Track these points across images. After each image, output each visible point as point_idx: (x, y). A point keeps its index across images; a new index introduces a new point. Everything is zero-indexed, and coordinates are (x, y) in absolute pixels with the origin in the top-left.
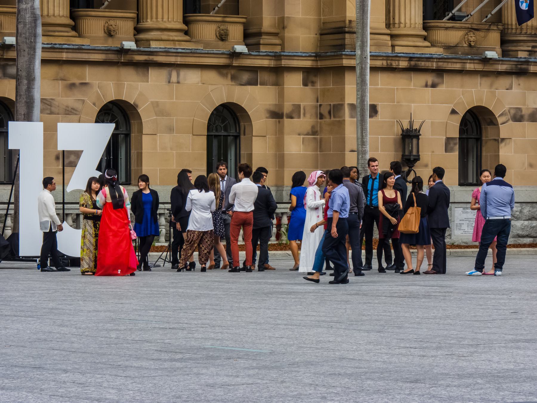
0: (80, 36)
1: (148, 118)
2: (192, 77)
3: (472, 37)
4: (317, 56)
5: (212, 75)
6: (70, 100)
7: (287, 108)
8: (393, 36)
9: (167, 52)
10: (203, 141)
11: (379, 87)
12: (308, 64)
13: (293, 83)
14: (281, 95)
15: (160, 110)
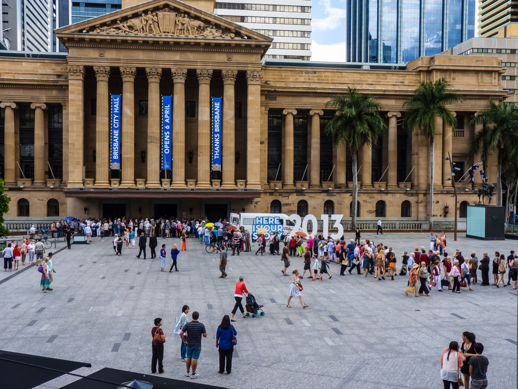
0: (373, 187)
1: (387, 204)
2: (398, 195)
3: (464, 186)
4: (426, 190)
5: (402, 195)
6: (370, 200)
7: (419, 201)
8: (443, 186)
9: (392, 190)
10: (400, 208)
11: (440, 197)
12: (424, 192)
13: (421, 197)
14: (418, 198)
15: (390, 202)
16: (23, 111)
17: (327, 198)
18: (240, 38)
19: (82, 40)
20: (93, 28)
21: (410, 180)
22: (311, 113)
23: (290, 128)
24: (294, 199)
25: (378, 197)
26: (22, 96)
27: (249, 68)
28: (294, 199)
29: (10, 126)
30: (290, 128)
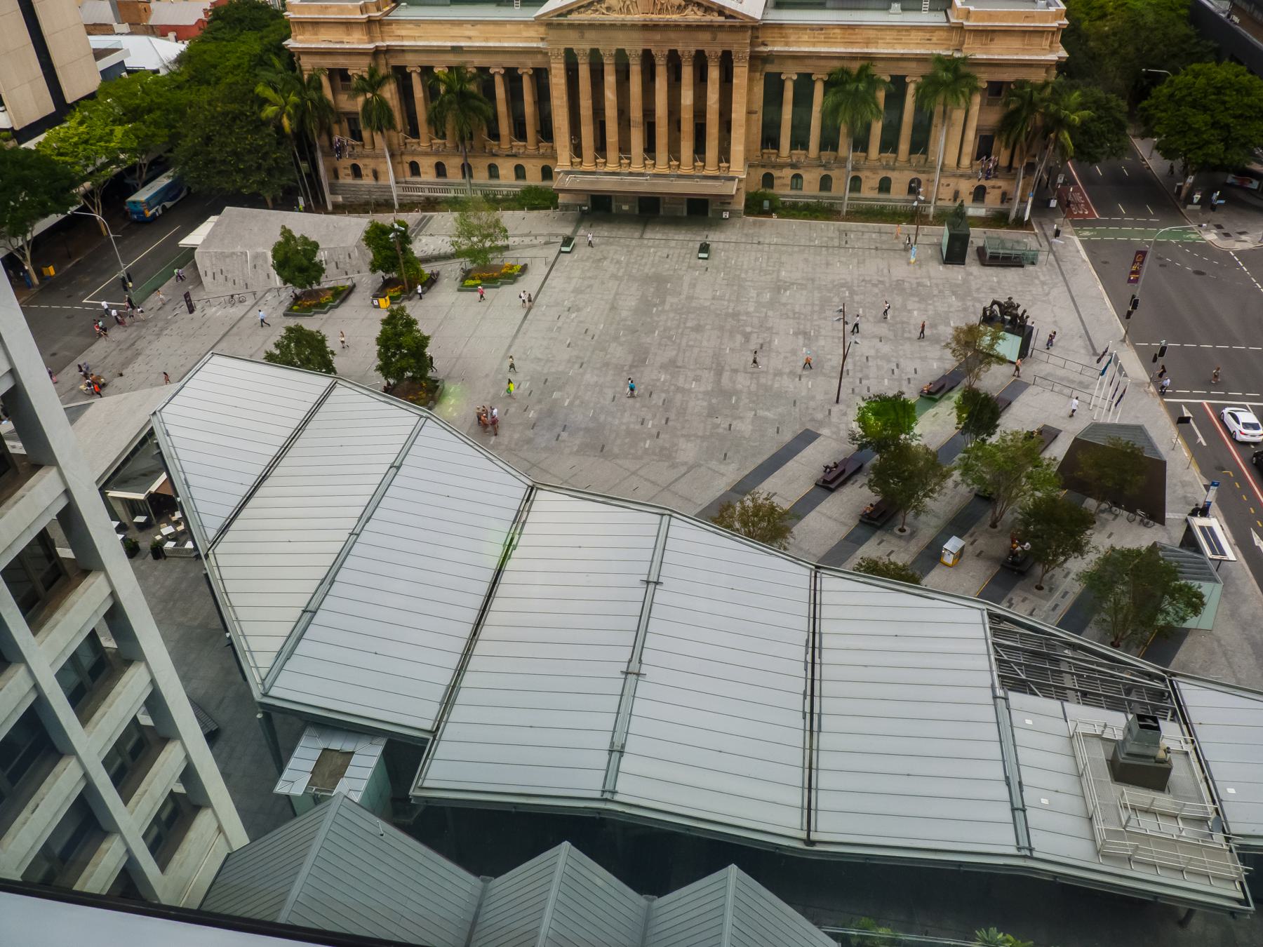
2: (906, 172)
16: (512, 77)
17: (825, 173)
18: (722, 19)
19: (560, 25)
20: (570, 12)
21: (925, 152)
22: (814, 78)
23: (789, 94)
24: (788, 173)
25: (883, 174)
26: (511, 62)
27: (734, 49)
28: (788, 173)
29: (500, 92)
30: (789, 94)
